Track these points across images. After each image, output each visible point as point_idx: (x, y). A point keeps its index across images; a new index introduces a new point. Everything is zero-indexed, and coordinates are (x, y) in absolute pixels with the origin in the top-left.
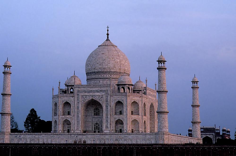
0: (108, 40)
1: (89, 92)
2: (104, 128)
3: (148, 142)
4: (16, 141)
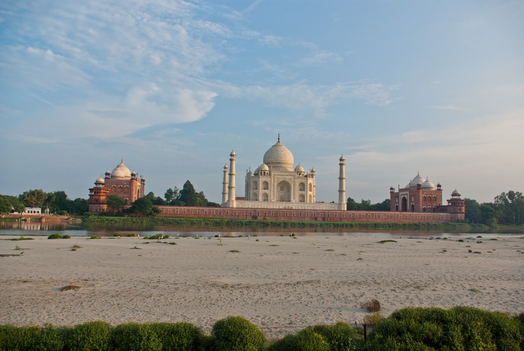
0: (279, 142)
1: (282, 175)
2: (292, 199)
3: (333, 209)
4: (240, 206)
